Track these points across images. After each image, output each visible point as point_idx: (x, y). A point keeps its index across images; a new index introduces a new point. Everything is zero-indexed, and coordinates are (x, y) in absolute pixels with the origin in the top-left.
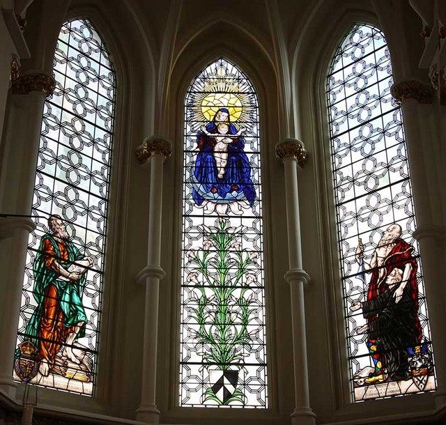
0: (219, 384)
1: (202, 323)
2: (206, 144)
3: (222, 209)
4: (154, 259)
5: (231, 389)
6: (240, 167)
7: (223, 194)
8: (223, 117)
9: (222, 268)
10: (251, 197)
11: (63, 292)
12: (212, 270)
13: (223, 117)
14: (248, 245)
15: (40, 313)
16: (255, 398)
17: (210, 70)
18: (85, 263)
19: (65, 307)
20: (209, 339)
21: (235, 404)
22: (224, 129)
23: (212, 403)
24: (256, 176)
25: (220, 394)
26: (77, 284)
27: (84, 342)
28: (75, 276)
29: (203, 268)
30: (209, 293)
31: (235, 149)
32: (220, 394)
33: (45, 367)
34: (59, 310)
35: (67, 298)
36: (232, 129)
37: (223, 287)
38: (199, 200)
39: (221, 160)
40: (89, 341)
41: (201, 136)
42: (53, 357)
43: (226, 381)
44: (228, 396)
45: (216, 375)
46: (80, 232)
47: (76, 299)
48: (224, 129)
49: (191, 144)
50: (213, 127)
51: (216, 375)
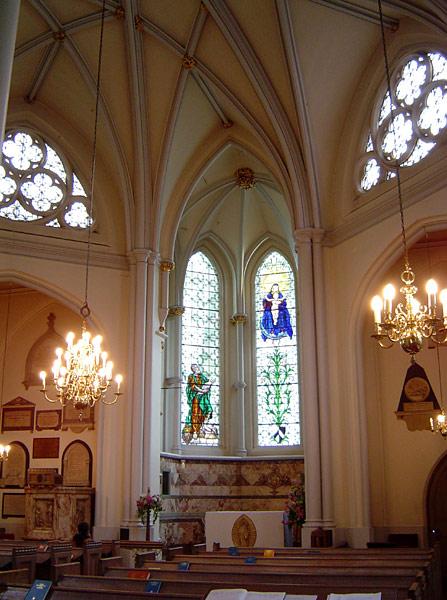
0: (278, 433)
1: (268, 404)
2: (268, 306)
3: (276, 343)
4: (241, 378)
5: (283, 436)
6: (285, 317)
7: (276, 334)
8: (275, 288)
9: (278, 375)
10: (291, 334)
11: (199, 400)
12: (271, 376)
13: (275, 288)
14: (289, 362)
15: (192, 412)
16: (293, 438)
17: (267, 260)
18: (209, 383)
19: (202, 406)
20: (272, 412)
21: (284, 443)
22: (276, 296)
23: (274, 444)
24: (293, 322)
25: (278, 438)
26: (206, 394)
27: (212, 421)
28: (205, 391)
29: (268, 376)
30: (271, 388)
31: (283, 307)
32: (278, 438)
33: (195, 435)
34: (199, 408)
35: (202, 402)
36: (280, 296)
37: (278, 385)
38: (265, 338)
39: (275, 314)
40: (215, 419)
41: (265, 301)
42: (198, 430)
43: (281, 433)
44: (281, 439)
45: (276, 429)
46: (206, 369)
47: (207, 401)
48: (276, 296)
49: (260, 307)
50: (271, 296)
51: (276, 429)
